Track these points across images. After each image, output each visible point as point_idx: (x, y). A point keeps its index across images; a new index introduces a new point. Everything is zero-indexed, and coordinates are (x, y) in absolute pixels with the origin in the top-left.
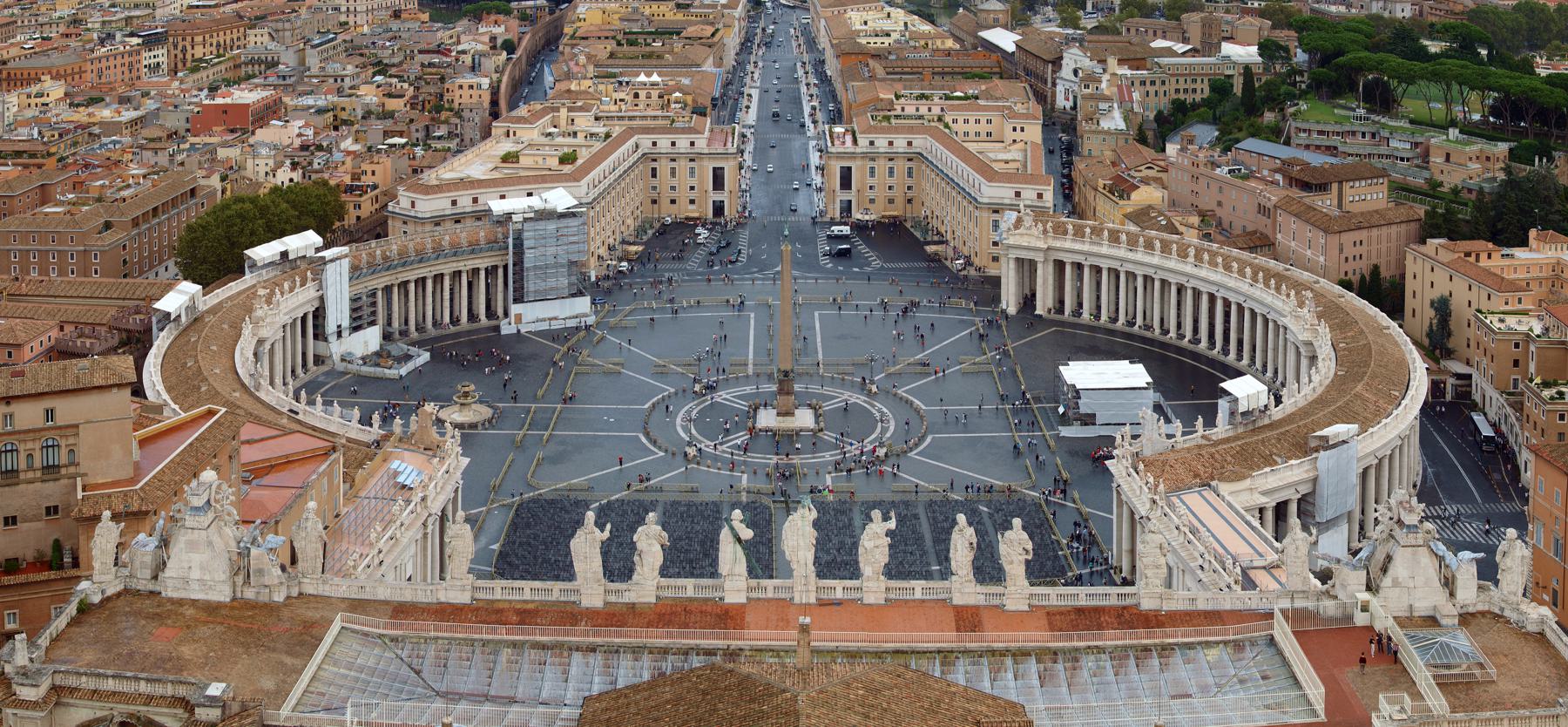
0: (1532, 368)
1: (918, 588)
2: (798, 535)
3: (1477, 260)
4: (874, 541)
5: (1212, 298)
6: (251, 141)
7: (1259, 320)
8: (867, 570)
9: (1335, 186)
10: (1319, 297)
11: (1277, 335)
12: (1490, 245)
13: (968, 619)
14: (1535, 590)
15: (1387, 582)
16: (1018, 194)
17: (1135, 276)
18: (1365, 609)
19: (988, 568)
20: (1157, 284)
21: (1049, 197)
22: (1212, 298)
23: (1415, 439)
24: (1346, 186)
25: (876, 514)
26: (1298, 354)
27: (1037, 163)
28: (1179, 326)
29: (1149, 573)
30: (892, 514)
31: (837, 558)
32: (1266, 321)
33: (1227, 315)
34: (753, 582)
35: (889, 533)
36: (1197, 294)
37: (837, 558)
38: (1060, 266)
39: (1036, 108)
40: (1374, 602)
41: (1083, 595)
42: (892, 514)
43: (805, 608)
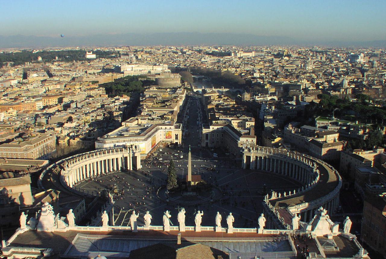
0: (370, 180)
1: (209, 229)
2: (182, 216)
3: (359, 154)
4: (199, 217)
5: (292, 165)
6: (64, 126)
7: (303, 170)
8: (197, 224)
9: (325, 136)
10: (317, 164)
11: (307, 173)
12: (362, 150)
13: (219, 235)
14: (351, 232)
15: (316, 228)
16: (247, 140)
17: (274, 160)
18: (310, 233)
19: (224, 224)
20: (279, 161)
21: (255, 140)
22: (292, 165)
23: (338, 198)
24: (328, 136)
25: (199, 212)
26: (311, 178)
27: (252, 132)
28: (284, 172)
29: (260, 225)
30: (202, 212)
31: (190, 221)
32: (305, 170)
33: (296, 168)
34: (171, 227)
35: (202, 216)
36: (289, 163)
37: (190, 221)
38: (257, 157)
39: (253, 119)
40: (313, 233)
41: (245, 230)
42: (202, 212)
43: (181, 232)
